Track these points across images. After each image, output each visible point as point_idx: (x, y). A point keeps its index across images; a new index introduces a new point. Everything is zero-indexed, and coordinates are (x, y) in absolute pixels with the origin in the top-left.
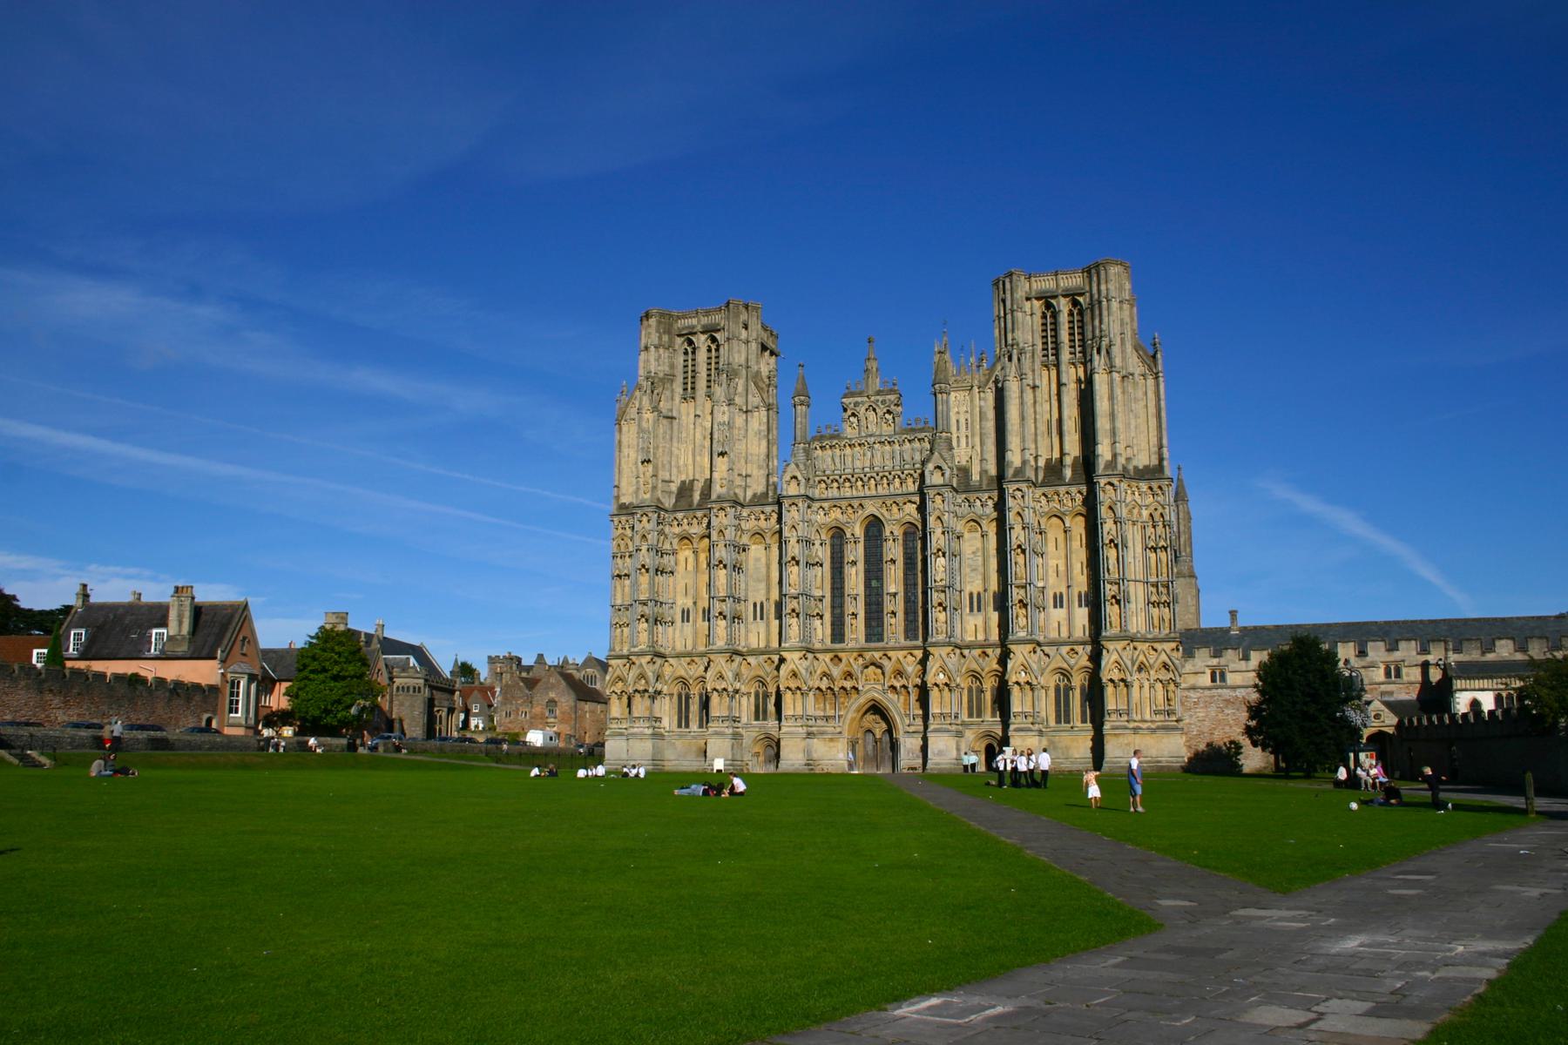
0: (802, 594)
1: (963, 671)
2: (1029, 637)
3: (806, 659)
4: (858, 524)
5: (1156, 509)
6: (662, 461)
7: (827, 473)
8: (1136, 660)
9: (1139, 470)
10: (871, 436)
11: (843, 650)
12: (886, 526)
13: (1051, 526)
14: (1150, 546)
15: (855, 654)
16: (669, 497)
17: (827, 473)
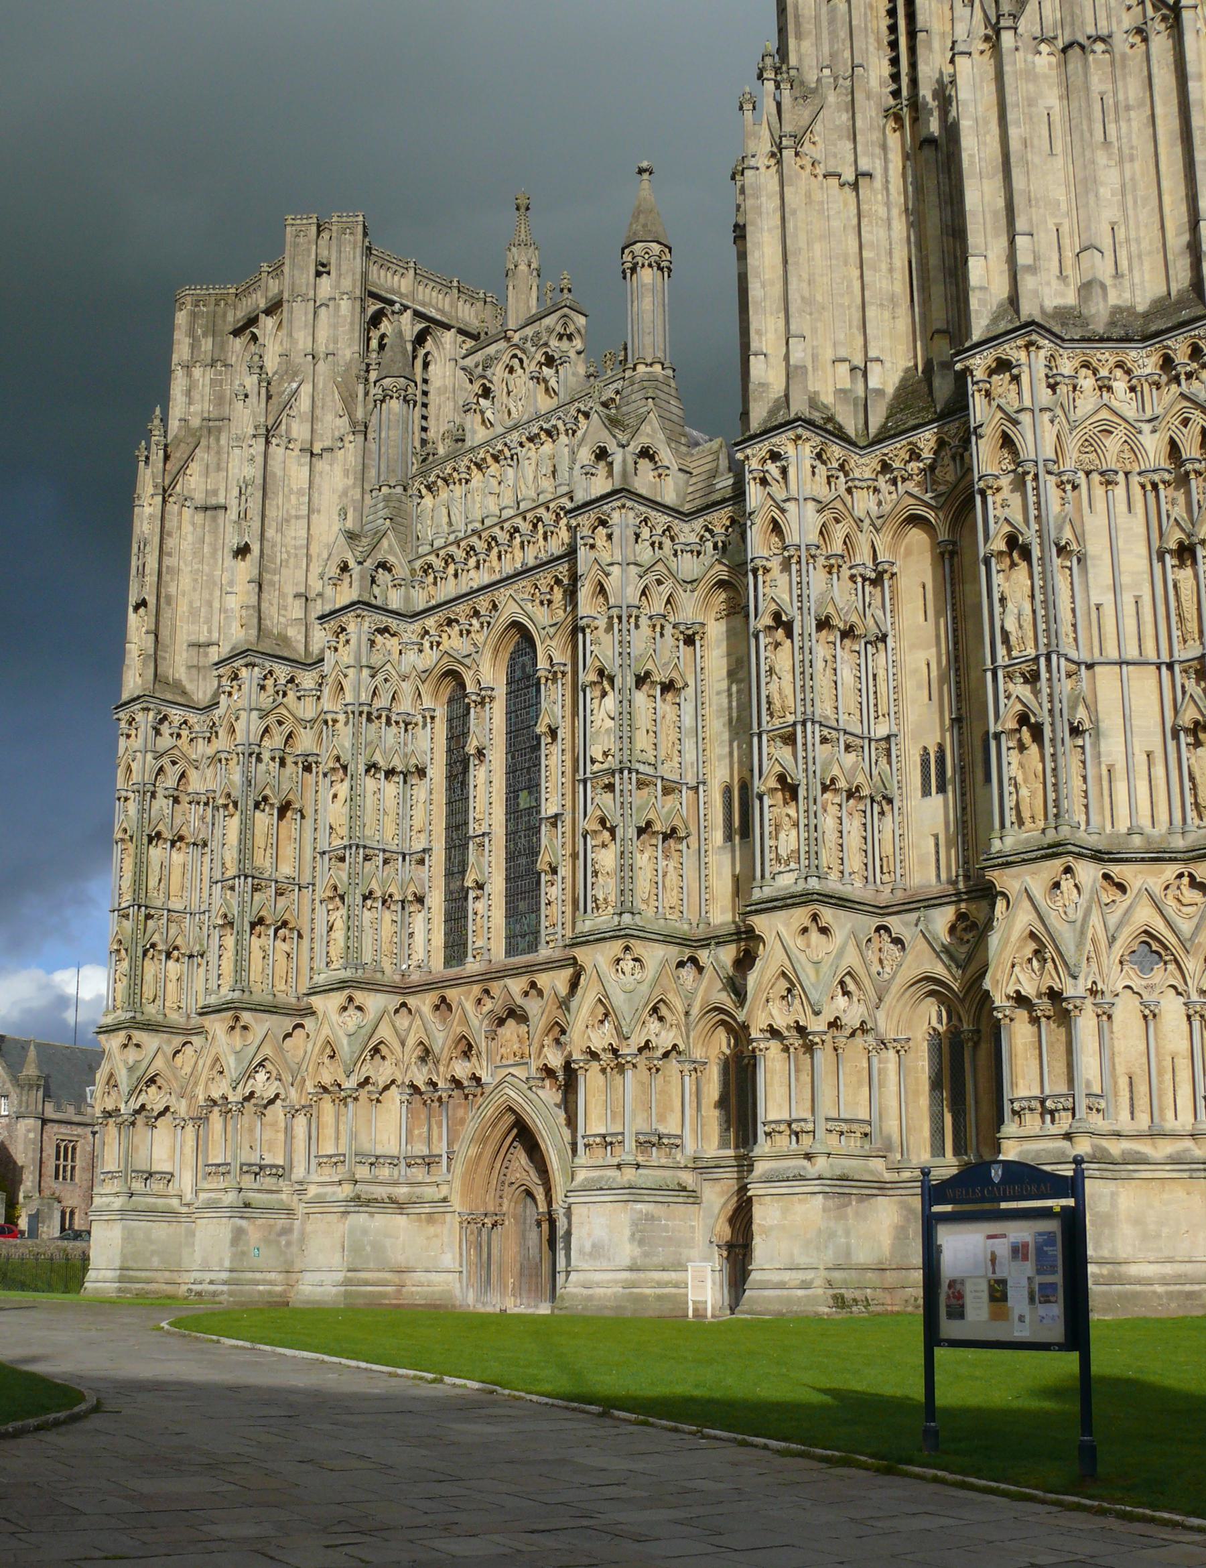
0: (350, 847)
1: (695, 1011)
2: (801, 887)
3: (359, 1008)
4: (488, 654)
5: (1186, 422)
6: (191, 602)
7: (436, 545)
8: (1120, 925)
9: (1137, 315)
10: (515, 427)
11: (456, 982)
12: (538, 643)
13: (908, 553)
14: (1173, 545)
15: (476, 989)
16: (204, 679)
17: (436, 545)
